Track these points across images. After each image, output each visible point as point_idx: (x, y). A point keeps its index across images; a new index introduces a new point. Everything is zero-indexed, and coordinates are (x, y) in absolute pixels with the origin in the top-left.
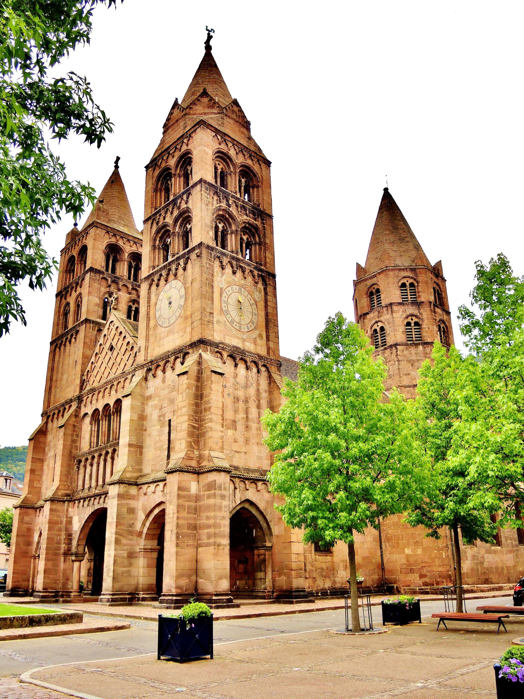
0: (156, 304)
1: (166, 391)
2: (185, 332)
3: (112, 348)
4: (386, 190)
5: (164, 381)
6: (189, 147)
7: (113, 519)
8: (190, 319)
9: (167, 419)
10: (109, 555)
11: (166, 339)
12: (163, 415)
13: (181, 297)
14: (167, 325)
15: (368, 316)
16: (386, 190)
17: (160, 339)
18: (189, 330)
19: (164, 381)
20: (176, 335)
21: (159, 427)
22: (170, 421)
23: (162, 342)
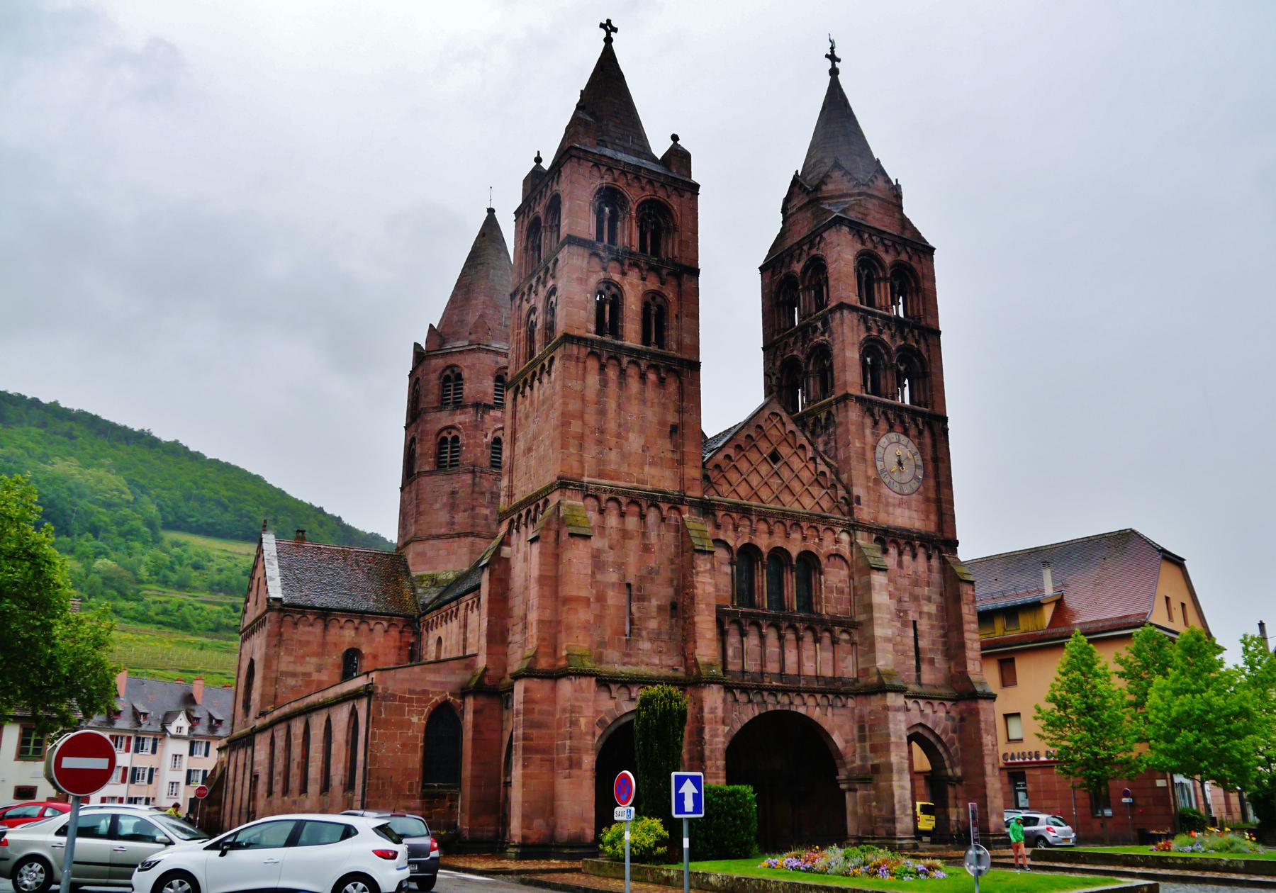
0: (874, 448)
1: (906, 582)
2: (928, 517)
3: (775, 457)
4: (491, 211)
5: (900, 564)
6: (914, 264)
7: (901, 738)
8: (933, 506)
9: (911, 619)
10: (903, 787)
11: (898, 511)
12: (906, 612)
13: (917, 466)
14: (897, 489)
15: (492, 413)
16: (491, 211)
17: (888, 504)
18: (933, 517)
19: (900, 564)
20: (915, 515)
21: (899, 625)
22: (915, 622)
23: (891, 509)
